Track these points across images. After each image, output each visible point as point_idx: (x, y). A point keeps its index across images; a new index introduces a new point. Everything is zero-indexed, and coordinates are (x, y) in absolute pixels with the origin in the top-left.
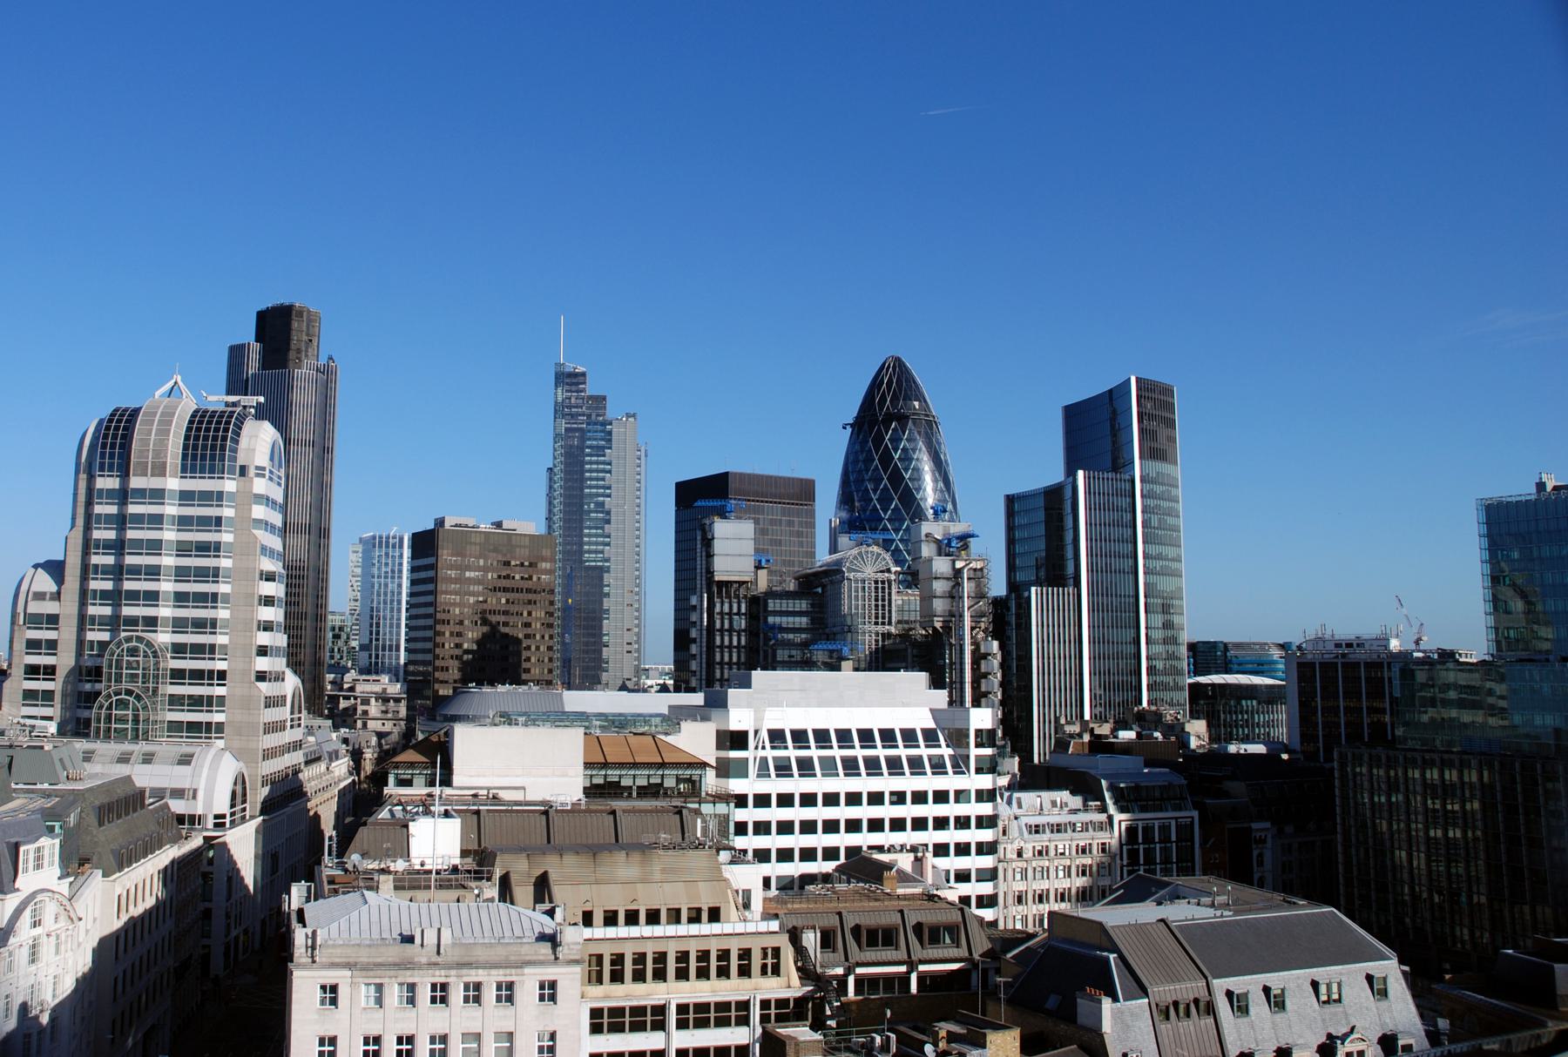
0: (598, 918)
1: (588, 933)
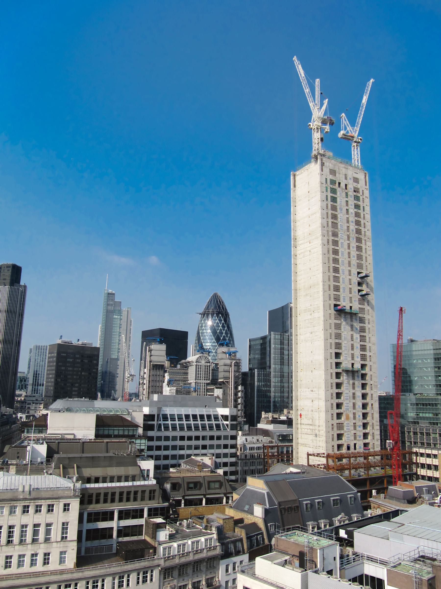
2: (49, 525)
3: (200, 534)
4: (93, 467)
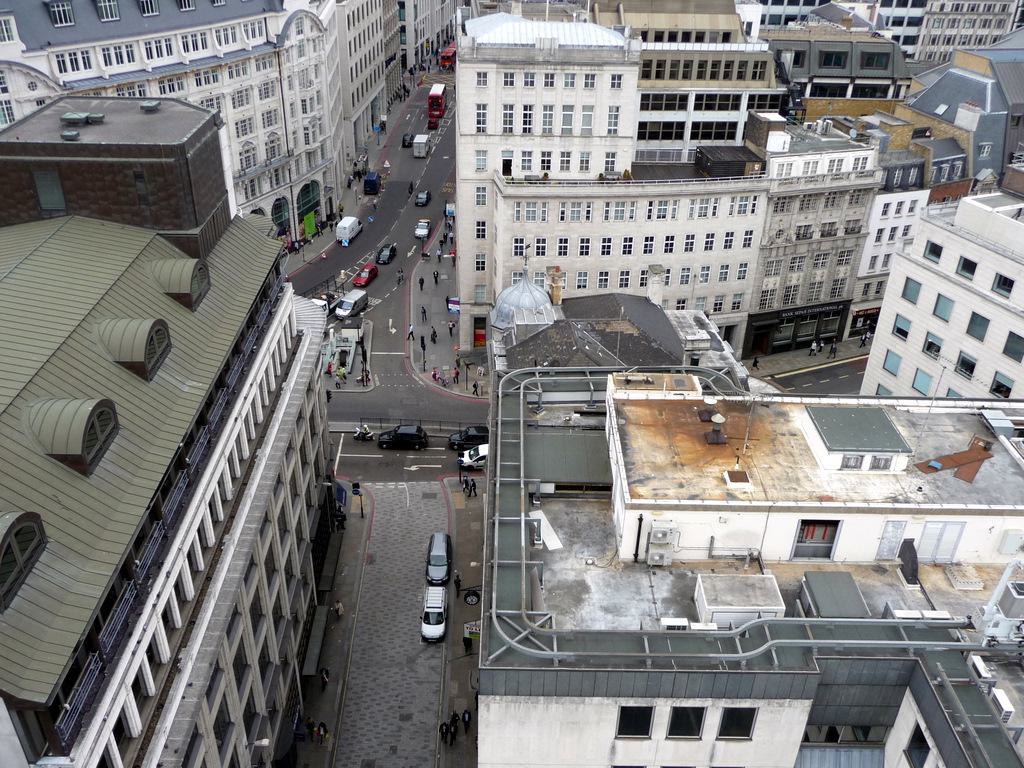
0: (651, 36)
1: (645, 46)
2: (589, 108)
3: (846, 146)
4: (652, 12)
